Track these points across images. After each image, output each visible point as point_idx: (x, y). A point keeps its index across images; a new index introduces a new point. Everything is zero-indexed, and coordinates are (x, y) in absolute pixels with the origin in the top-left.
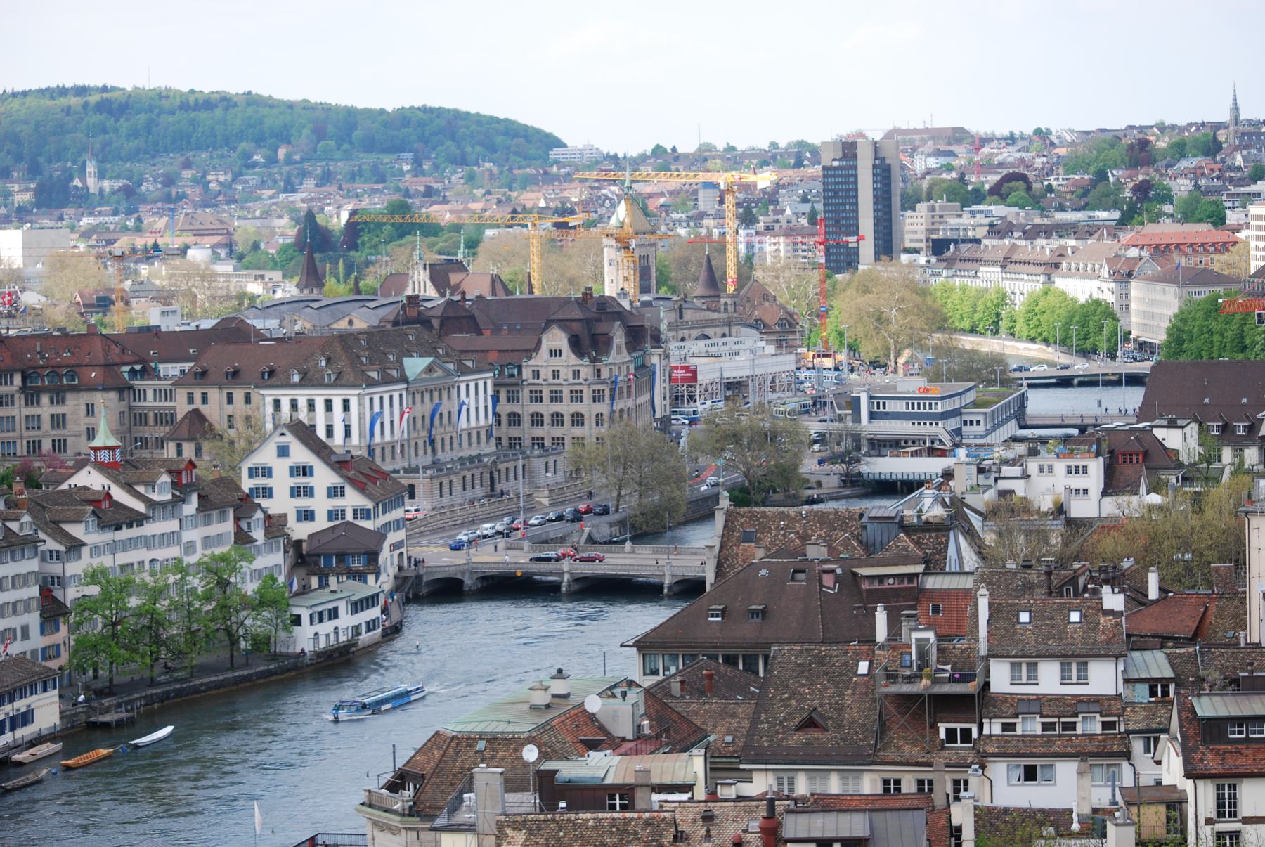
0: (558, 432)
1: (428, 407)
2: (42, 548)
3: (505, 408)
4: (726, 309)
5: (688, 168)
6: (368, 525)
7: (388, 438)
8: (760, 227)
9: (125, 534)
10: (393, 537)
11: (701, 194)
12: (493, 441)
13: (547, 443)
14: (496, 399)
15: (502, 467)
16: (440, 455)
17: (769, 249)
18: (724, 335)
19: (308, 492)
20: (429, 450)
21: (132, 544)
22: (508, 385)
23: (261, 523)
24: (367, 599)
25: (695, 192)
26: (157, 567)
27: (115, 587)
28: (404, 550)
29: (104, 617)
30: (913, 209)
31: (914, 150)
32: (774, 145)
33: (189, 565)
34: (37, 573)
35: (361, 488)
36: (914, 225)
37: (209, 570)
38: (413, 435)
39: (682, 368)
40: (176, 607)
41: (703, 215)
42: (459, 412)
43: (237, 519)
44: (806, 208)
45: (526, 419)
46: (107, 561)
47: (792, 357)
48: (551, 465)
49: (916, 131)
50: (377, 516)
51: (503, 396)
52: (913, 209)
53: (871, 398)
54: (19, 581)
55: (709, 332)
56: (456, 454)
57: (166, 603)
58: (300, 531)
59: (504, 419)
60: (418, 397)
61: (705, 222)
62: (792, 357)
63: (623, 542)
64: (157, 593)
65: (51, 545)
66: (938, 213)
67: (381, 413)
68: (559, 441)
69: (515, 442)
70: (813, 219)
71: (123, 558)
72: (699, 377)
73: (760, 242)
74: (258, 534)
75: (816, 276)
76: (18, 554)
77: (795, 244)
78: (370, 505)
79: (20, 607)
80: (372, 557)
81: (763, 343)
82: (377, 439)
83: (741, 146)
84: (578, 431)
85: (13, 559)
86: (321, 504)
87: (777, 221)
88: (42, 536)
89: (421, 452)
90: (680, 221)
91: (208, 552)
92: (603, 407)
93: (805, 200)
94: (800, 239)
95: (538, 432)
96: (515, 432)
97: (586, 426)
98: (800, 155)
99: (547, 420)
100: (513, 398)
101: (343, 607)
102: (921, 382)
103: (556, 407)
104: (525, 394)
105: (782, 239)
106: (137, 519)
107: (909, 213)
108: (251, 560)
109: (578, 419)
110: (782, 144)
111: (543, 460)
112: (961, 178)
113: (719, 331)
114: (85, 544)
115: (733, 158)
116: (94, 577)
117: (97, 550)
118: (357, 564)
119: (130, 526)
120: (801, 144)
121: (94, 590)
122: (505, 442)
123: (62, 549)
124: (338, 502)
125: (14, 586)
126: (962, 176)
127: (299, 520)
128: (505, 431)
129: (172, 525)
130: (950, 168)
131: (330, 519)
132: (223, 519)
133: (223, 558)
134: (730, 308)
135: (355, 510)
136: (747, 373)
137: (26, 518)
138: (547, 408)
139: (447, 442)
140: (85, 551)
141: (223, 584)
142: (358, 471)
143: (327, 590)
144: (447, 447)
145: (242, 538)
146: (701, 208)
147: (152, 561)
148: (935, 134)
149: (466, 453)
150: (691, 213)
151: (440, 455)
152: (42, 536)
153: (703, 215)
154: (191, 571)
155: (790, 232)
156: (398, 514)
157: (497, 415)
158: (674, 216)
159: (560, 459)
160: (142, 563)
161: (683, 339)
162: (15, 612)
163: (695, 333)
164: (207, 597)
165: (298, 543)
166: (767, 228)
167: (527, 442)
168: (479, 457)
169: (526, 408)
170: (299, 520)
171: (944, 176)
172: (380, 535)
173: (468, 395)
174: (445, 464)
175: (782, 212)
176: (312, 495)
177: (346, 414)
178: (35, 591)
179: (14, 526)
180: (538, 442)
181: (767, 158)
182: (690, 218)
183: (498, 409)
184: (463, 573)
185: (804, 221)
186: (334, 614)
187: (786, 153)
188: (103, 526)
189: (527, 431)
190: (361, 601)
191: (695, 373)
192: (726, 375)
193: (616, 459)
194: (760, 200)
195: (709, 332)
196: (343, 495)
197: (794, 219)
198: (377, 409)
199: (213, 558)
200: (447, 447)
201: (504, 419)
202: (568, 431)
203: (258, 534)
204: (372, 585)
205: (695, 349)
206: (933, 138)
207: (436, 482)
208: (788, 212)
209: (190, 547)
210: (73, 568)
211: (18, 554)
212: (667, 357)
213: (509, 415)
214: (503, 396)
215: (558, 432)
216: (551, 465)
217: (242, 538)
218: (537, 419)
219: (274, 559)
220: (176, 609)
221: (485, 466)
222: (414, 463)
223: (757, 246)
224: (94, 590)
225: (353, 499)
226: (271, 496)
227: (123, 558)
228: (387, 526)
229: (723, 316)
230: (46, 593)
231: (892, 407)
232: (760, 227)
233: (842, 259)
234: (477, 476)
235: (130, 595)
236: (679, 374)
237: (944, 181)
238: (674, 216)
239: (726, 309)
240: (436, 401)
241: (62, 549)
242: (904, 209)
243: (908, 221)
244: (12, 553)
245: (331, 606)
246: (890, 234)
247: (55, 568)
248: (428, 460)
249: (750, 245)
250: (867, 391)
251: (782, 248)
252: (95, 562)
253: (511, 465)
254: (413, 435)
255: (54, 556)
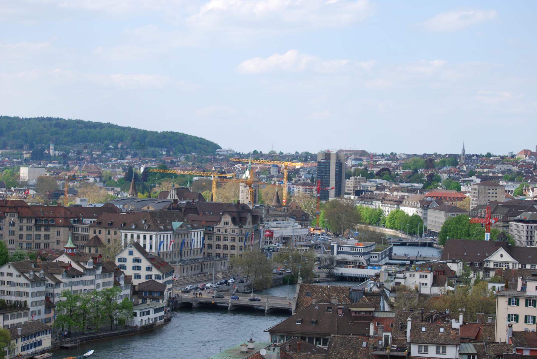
0: (226, 252)
1: (180, 241)
2: (47, 282)
3: (207, 242)
4: (284, 211)
5: (266, 159)
6: (160, 281)
7: (165, 250)
8: (293, 182)
9: (76, 279)
10: (169, 286)
11: (271, 170)
12: (202, 254)
13: (221, 256)
14: (204, 239)
15: (206, 263)
16: (183, 258)
17: (296, 190)
18: (283, 220)
19: (139, 268)
20: (180, 256)
21: (78, 283)
22: (208, 234)
23: (123, 279)
24: (160, 308)
25: (270, 168)
26: (86, 292)
27: (72, 297)
28: (171, 291)
29: (68, 309)
30: (349, 179)
31: (348, 157)
32: (297, 153)
33: (99, 292)
34: (44, 292)
35: (158, 268)
36: (349, 184)
37: (105, 295)
38: (174, 250)
39: (268, 231)
40: (93, 307)
41: (273, 176)
42: (191, 243)
43: (115, 277)
44: (310, 176)
45: (214, 246)
46: (69, 288)
47: (308, 230)
48: (223, 263)
49: (348, 151)
50: (163, 278)
51: (206, 238)
52: (349, 179)
53: (338, 246)
54: (38, 294)
55: (278, 219)
56: (189, 258)
57: (90, 305)
58: (136, 282)
59: (206, 246)
60: (177, 236)
61: (273, 179)
62: (308, 230)
63: (250, 293)
64: (86, 302)
65: (50, 282)
66: (358, 180)
67: (163, 241)
68: (225, 255)
69: (209, 255)
70: (312, 180)
71: (75, 288)
72: (274, 235)
73: (293, 187)
74: (122, 283)
75: (315, 200)
76: (38, 285)
77: (306, 189)
78: (161, 275)
79: (38, 303)
80: (162, 293)
81: (297, 224)
82: (162, 251)
83: (285, 153)
84: (233, 252)
85: (37, 286)
86: (143, 273)
87: (299, 180)
88: (47, 278)
89: (177, 256)
90: (264, 178)
91: (105, 288)
92: (242, 244)
93: (309, 173)
94: (307, 187)
95: (218, 251)
96: (210, 251)
97: (236, 251)
98: (306, 157)
99: (222, 247)
100: (210, 238)
101: (151, 311)
102: (357, 241)
103: (226, 243)
104: (214, 237)
105: (301, 187)
106: (80, 275)
107: (347, 180)
108: (120, 292)
109: (233, 248)
110: (300, 153)
111: (220, 262)
112: (366, 169)
113: (281, 218)
114: (62, 282)
115: (282, 157)
116: (65, 294)
117: (66, 285)
118: (156, 295)
119: (78, 277)
120: (307, 153)
121: (65, 299)
122: (206, 254)
123: (54, 283)
124: (149, 273)
125: (36, 296)
126: (366, 167)
127: (135, 278)
128: (206, 250)
129: (92, 277)
130: (361, 165)
131: (146, 278)
132: (110, 276)
133: (111, 290)
134: (286, 211)
135: (155, 276)
136: (291, 234)
137: (42, 272)
138: (222, 243)
139: (186, 253)
140: (62, 285)
141: (109, 299)
142: (156, 261)
143: (146, 304)
144: (186, 255)
145: (116, 283)
146: (272, 174)
147: (85, 290)
148: (355, 152)
149: (192, 258)
150: (268, 176)
151: (183, 258)
152: (47, 278)
153: (273, 176)
154: (99, 294)
155: (304, 184)
156: (170, 278)
157: (204, 244)
158: (262, 176)
159: (226, 261)
160: (81, 290)
161: (268, 221)
162: (36, 305)
163: (273, 219)
164: (104, 304)
165: (135, 286)
166: (296, 182)
167: (214, 255)
168: (197, 259)
169: (215, 242)
170: (135, 278)
171: (359, 167)
172: (164, 285)
173: (194, 237)
174: (185, 261)
175: (301, 177)
176: (140, 269)
177: (151, 240)
178: (43, 298)
179: (38, 274)
180: (218, 255)
181: (295, 158)
182: (268, 177)
183: (204, 242)
184: (193, 301)
185: (309, 181)
186: (148, 313)
187: (301, 156)
188: (68, 276)
189: (214, 251)
190: (158, 309)
191: (272, 233)
192: (284, 235)
193: (247, 263)
194: (293, 172)
195: (278, 219)
196: (151, 270)
197: (305, 180)
198: (162, 240)
199: (107, 290)
200: (186, 255)
201: (206, 246)
202: (228, 251)
203: (122, 283)
204: (163, 303)
205: (272, 225)
206: (354, 154)
207: (182, 267)
208: (303, 177)
209: (98, 286)
210: (57, 291)
211: (38, 285)
212: (264, 227)
213: (208, 245)
214: (206, 238)
215: (226, 252)
216: (223, 263)
217: (116, 283)
218: (218, 247)
219: (128, 292)
220: (93, 308)
221: (199, 263)
222: (174, 260)
223: (292, 189)
224: (65, 299)
225: (155, 272)
226: (125, 269)
227: (75, 288)
228: (166, 282)
229: (283, 213)
230: (47, 299)
231: (346, 249)
232: (293, 182)
233: (325, 195)
234: (197, 266)
235: (77, 302)
236: (267, 233)
237: (360, 169)
238: (262, 176)
239: (284, 211)
240: (183, 238)
241: (54, 283)
242: (346, 179)
243: (347, 183)
244: (37, 284)
245: (147, 310)
246: (341, 187)
247: (51, 290)
248: (179, 259)
249: (289, 188)
250: (337, 243)
251: (301, 190)
252: (66, 289)
253: (209, 263)
254: (174, 250)
255: (51, 286)
